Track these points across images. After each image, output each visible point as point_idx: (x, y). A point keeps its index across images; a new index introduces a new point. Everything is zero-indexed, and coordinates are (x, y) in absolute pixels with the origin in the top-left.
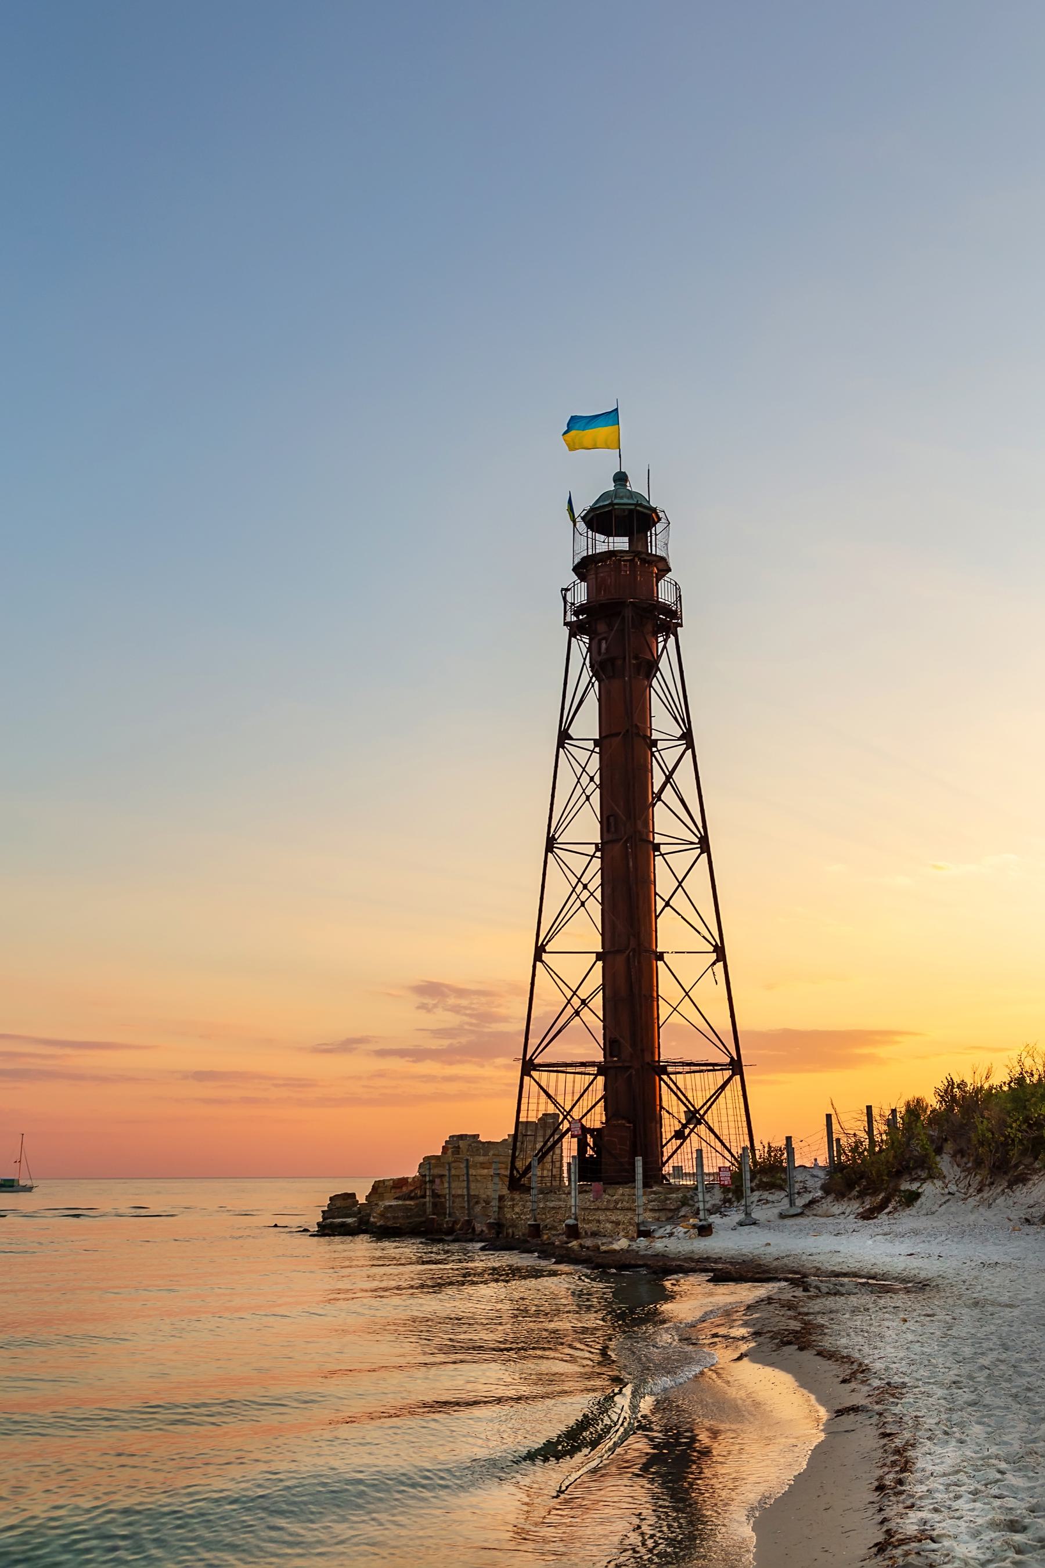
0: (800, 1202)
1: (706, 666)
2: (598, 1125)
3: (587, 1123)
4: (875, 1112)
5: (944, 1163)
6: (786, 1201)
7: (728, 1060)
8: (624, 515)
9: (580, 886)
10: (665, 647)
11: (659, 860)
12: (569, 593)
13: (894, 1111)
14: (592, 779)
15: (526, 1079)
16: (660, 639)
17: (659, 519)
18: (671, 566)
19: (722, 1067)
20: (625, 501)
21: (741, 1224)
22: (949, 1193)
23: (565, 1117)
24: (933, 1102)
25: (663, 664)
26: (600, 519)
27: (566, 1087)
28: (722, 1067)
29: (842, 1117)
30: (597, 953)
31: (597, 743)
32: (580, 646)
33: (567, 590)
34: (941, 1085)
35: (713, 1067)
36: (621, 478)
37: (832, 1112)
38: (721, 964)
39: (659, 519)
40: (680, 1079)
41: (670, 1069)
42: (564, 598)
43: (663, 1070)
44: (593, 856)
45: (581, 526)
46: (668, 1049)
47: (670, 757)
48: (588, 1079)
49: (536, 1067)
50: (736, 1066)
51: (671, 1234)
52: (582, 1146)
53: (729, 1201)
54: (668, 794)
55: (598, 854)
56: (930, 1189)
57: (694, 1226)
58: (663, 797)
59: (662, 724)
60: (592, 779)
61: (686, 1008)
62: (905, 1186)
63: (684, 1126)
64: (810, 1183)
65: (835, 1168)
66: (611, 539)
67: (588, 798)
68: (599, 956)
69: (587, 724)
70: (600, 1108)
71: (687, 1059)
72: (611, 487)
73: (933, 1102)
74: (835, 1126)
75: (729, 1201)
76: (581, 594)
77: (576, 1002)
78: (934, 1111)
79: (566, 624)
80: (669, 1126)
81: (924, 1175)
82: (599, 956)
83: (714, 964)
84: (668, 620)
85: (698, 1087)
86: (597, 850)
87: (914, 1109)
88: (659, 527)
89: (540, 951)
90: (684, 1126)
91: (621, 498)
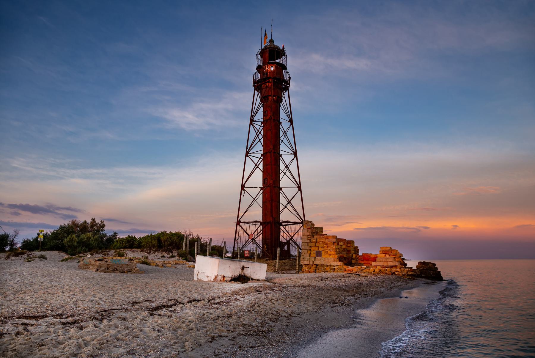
8: (272, 54)
15: (238, 226)
25: (284, 100)
35: (297, 223)
41: (283, 224)
44: (260, 158)
48: (257, 227)
60: (260, 133)
68: (262, 189)
69: (260, 116)
76: (258, 76)
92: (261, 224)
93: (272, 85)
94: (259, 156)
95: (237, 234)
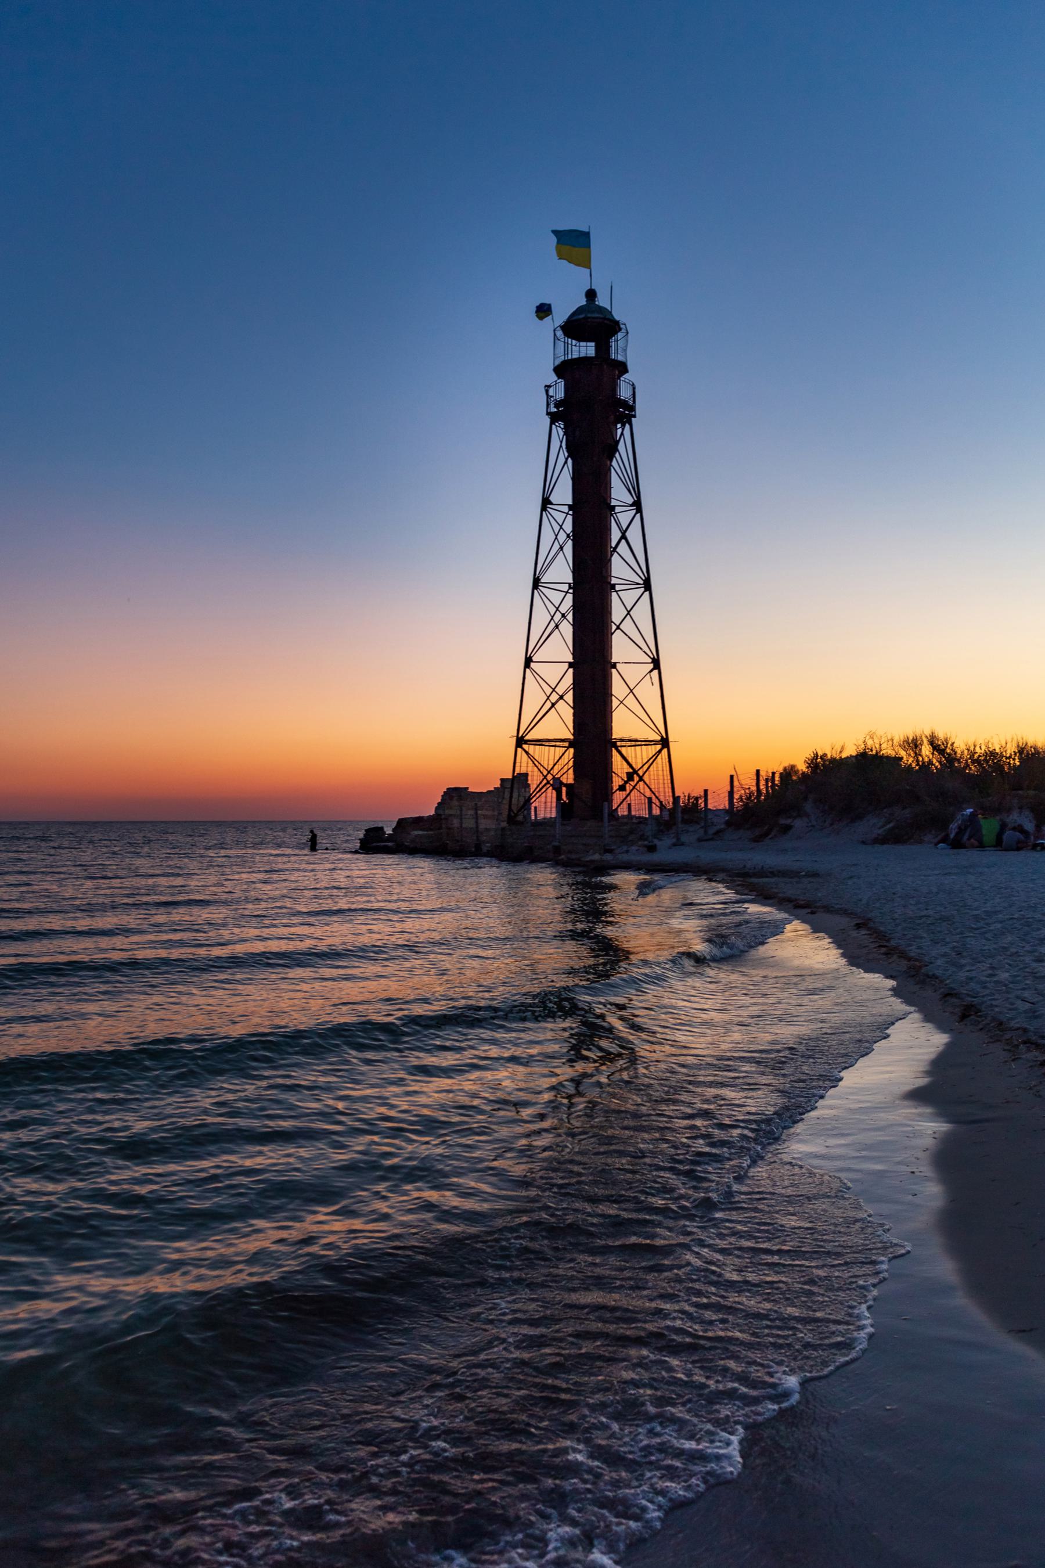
0: (711, 831)
1: (652, 448)
2: (571, 781)
3: (564, 780)
4: (762, 773)
5: (808, 807)
6: (702, 831)
7: (659, 738)
8: (593, 324)
9: (558, 616)
10: (622, 434)
11: (614, 594)
12: (551, 392)
13: (774, 773)
14: (568, 536)
15: (519, 750)
16: (619, 426)
17: (620, 329)
18: (629, 368)
19: (655, 743)
20: (596, 315)
21: (675, 845)
22: (813, 826)
23: (545, 777)
24: (802, 767)
25: (621, 447)
26: (574, 328)
27: (547, 756)
28: (655, 743)
29: (741, 778)
30: (570, 663)
31: (570, 507)
32: (558, 431)
33: (549, 386)
34: (808, 754)
36: (591, 294)
37: (733, 773)
38: (656, 672)
39: (620, 329)
40: (623, 750)
41: (619, 744)
42: (547, 392)
43: (614, 745)
44: (567, 592)
45: (560, 333)
46: (619, 730)
47: (624, 518)
49: (527, 742)
50: (665, 742)
51: (627, 852)
52: (559, 797)
53: (662, 831)
54: (623, 548)
55: (571, 591)
56: (798, 824)
57: (645, 846)
58: (618, 550)
59: (619, 494)
61: (630, 701)
62: (782, 821)
63: (626, 782)
64: (715, 820)
65: (730, 810)
66: (582, 344)
67: (561, 548)
68: (571, 665)
69: (563, 493)
70: (571, 771)
71: (634, 737)
72: (583, 302)
73: (802, 767)
74: (736, 783)
75: (662, 831)
77: (554, 697)
78: (803, 773)
79: (548, 414)
80: (617, 782)
81: (795, 814)
82: (571, 665)
83: (651, 671)
84: (625, 412)
85: (638, 756)
86: (570, 588)
87: (788, 773)
88: (620, 335)
89: (528, 661)
90: (626, 782)
91: (593, 312)
92: (572, 744)
93: (591, 411)
94: (565, 588)
95: (518, 764)
